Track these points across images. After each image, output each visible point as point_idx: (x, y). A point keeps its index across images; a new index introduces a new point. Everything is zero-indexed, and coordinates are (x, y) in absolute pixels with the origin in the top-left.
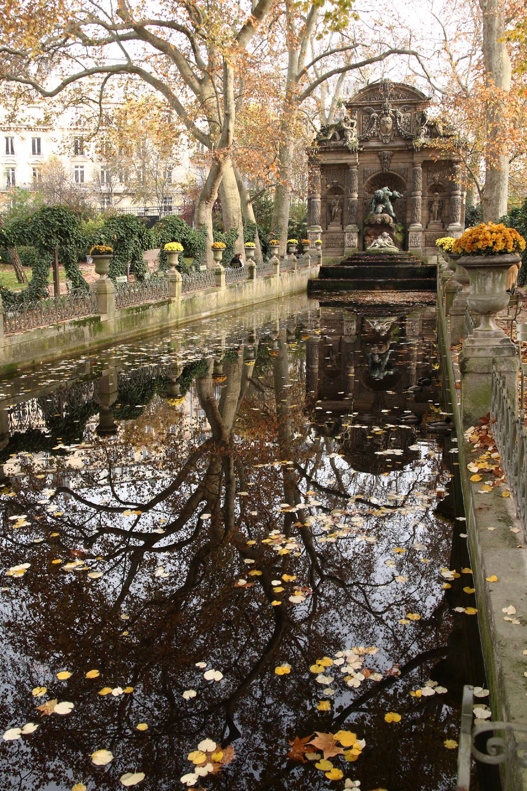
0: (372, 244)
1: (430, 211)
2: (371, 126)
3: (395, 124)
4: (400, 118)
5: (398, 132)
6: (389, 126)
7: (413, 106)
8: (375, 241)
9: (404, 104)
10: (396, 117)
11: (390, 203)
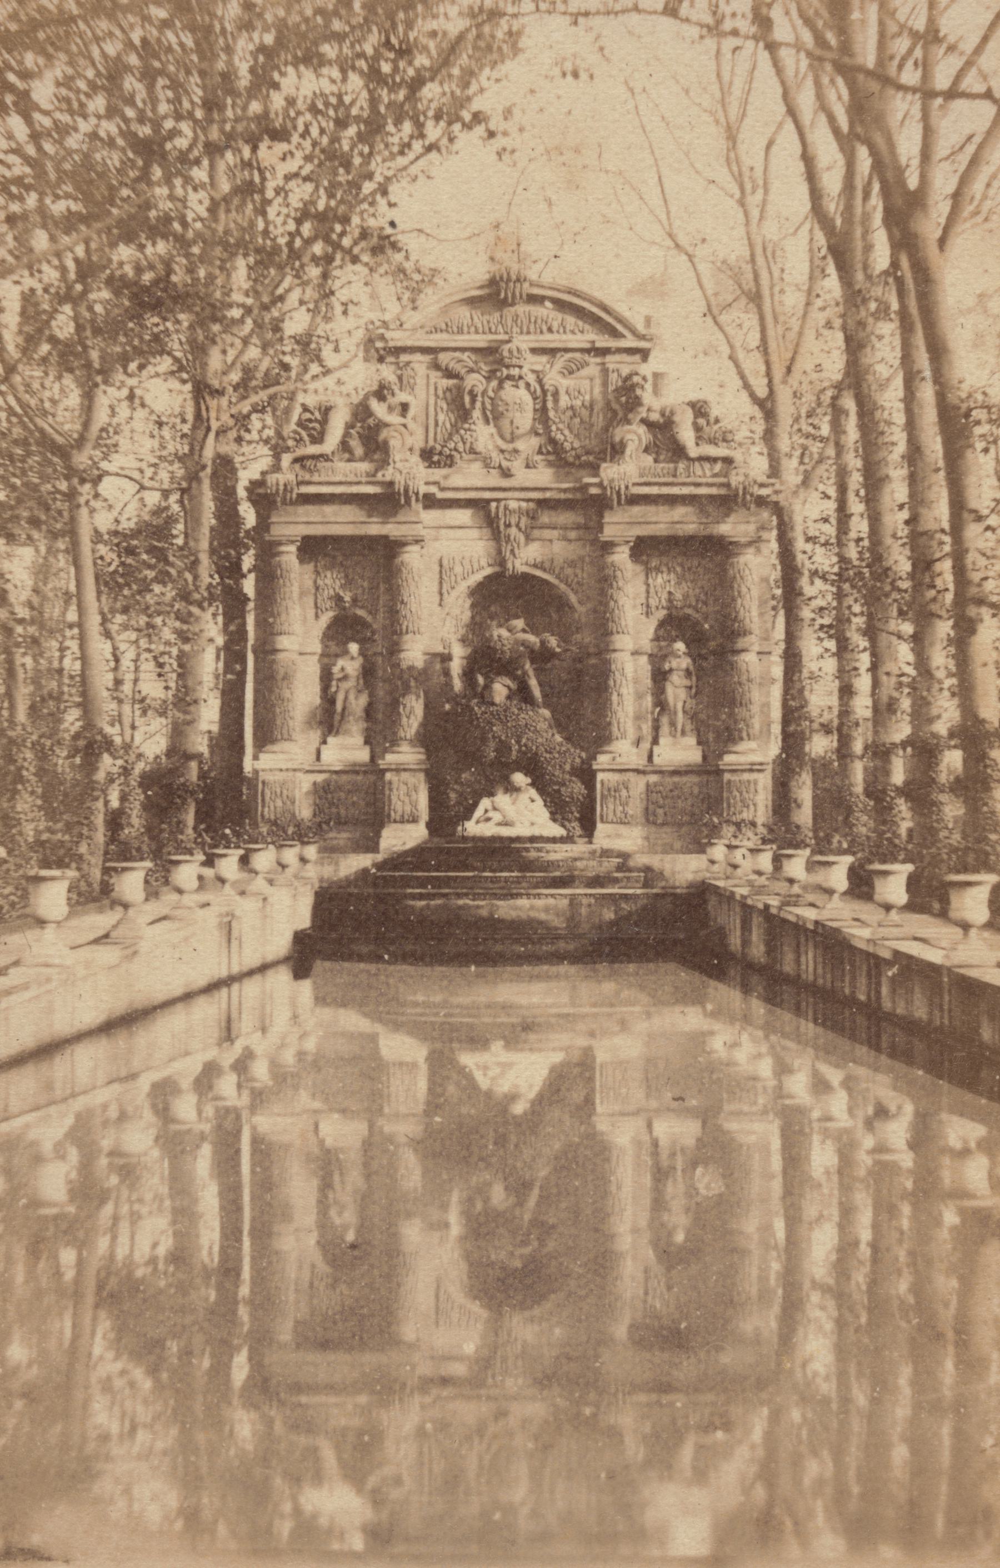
0: (479, 813)
1: (661, 704)
2: (464, 415)
3: (542, 413)
4: (556, 394)
5: (552, 441)
6: (525, 420)
7: (598, 360)
8: (485, 803)
9: (566, 350)
10: (544, 392)
11: (531, 673)
